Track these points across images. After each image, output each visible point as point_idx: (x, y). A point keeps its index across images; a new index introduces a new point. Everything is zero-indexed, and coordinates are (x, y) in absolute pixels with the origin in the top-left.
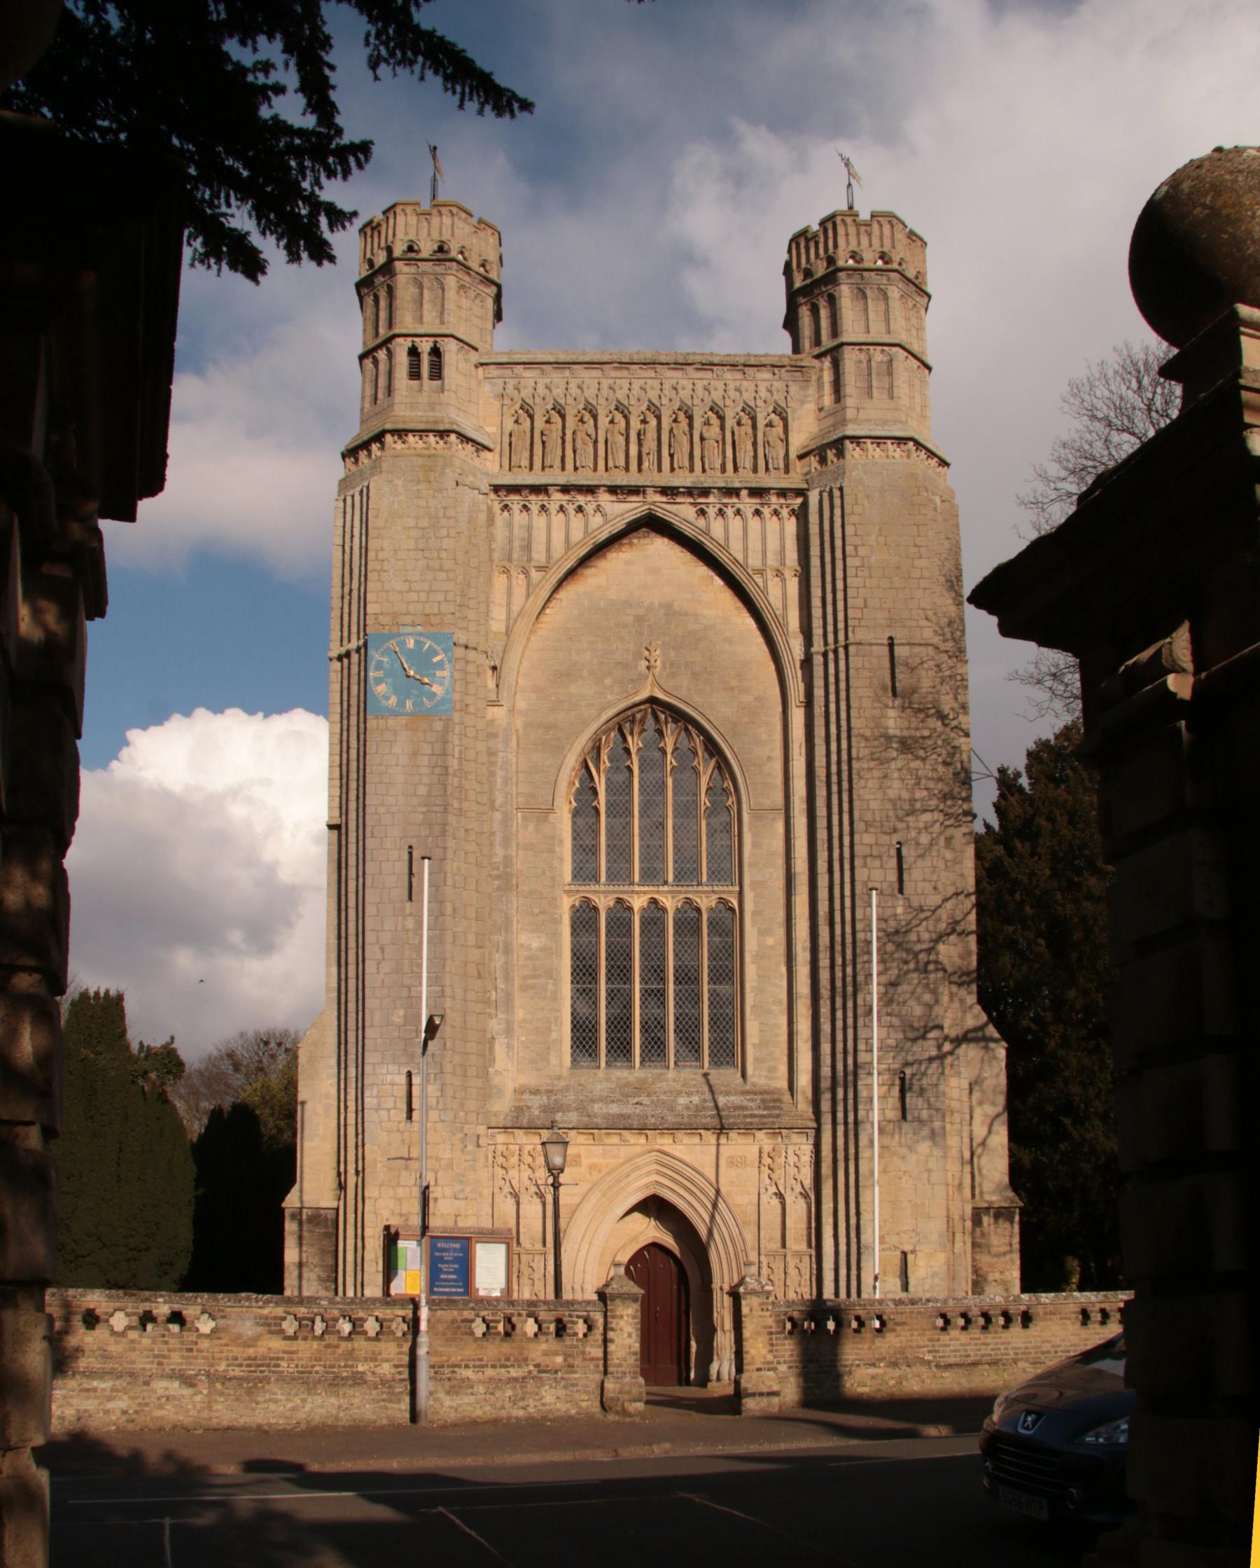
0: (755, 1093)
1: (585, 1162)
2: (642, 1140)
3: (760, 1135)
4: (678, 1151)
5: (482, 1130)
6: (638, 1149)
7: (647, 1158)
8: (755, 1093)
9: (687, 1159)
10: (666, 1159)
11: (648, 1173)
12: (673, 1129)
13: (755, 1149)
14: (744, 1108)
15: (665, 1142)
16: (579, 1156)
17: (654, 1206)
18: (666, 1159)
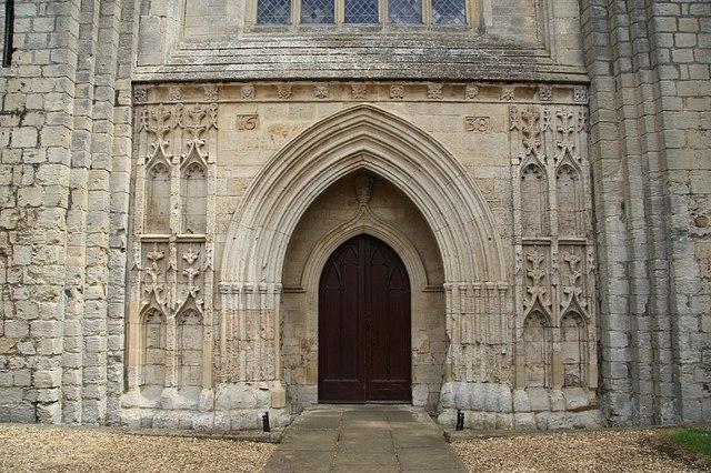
0: (498, 47)
1: (264, 124)
2: (345, 97)
3: (508, 90)
4: (396, 109)
5: (125, 85)
6: (340, 108)
7: (352, 119)
8: (498, 47)
9: (409, 119)
10: (379, 121)
11: (353, 141)
12: (385, 82)
13: (503, 109)
14: (484, 59)
15: (380, 101)
16: (256, 117)
17: (362, 184)
18: (379, 121)
